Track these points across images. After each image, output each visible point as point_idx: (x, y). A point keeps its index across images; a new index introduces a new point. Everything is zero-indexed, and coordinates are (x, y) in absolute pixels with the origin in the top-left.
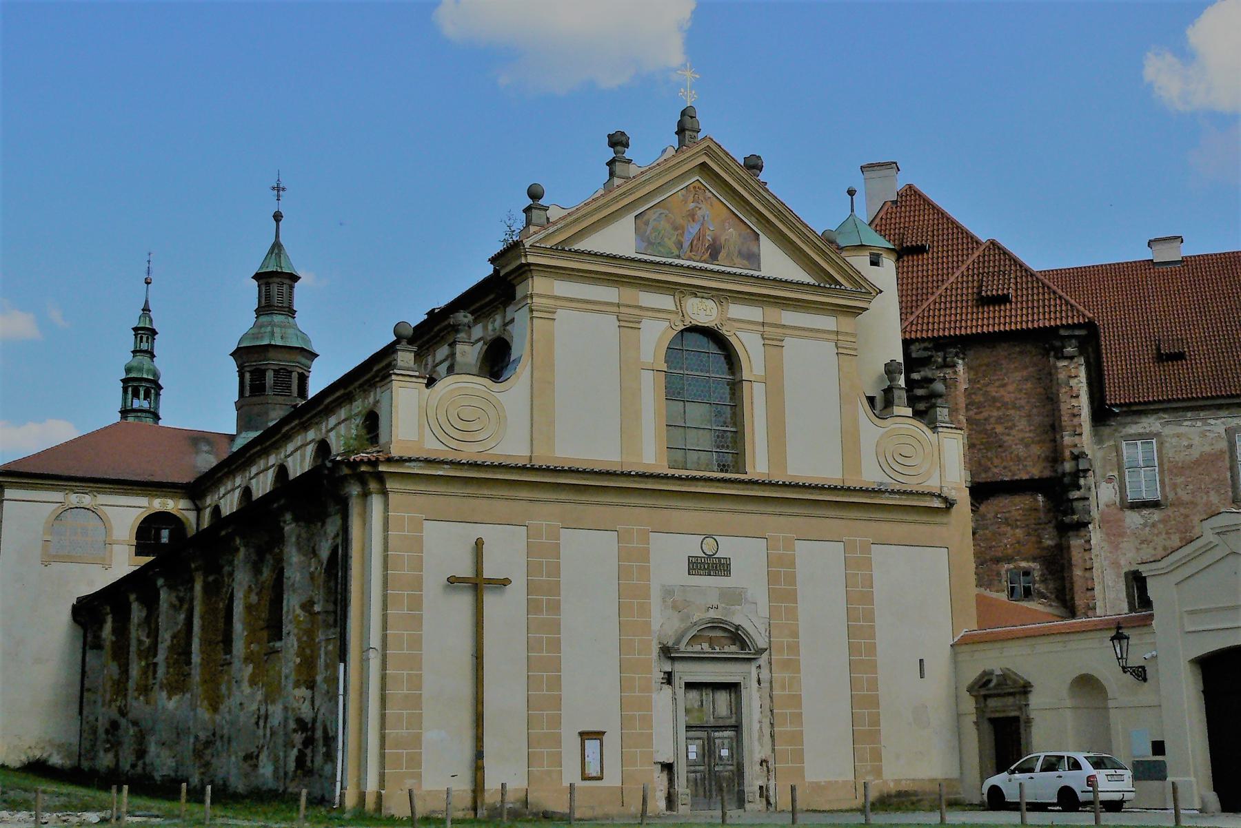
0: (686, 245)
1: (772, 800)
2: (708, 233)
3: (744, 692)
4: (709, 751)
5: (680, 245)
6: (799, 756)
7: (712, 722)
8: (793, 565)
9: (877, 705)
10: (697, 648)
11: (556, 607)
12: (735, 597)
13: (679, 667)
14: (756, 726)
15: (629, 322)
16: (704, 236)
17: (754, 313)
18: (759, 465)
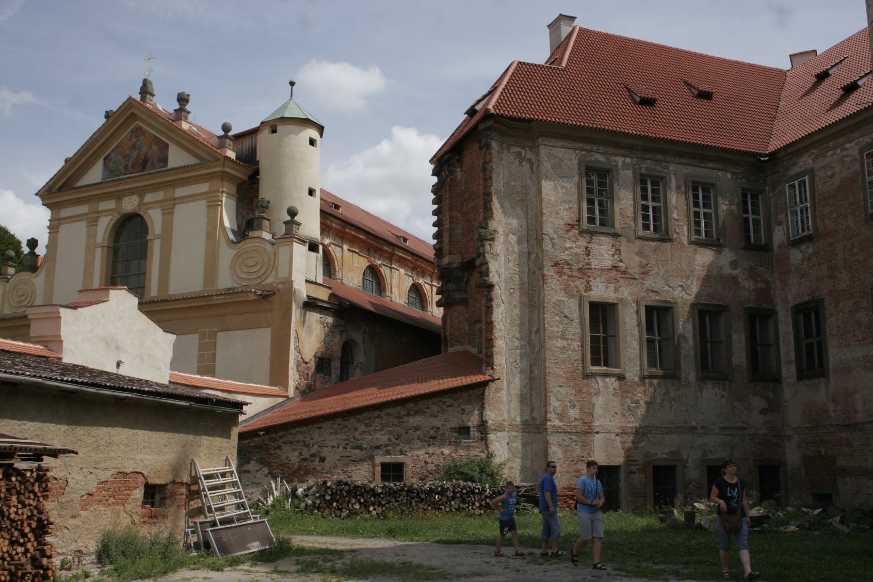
0: (130, 165)
15: (92, 223)
17: (160, 195)
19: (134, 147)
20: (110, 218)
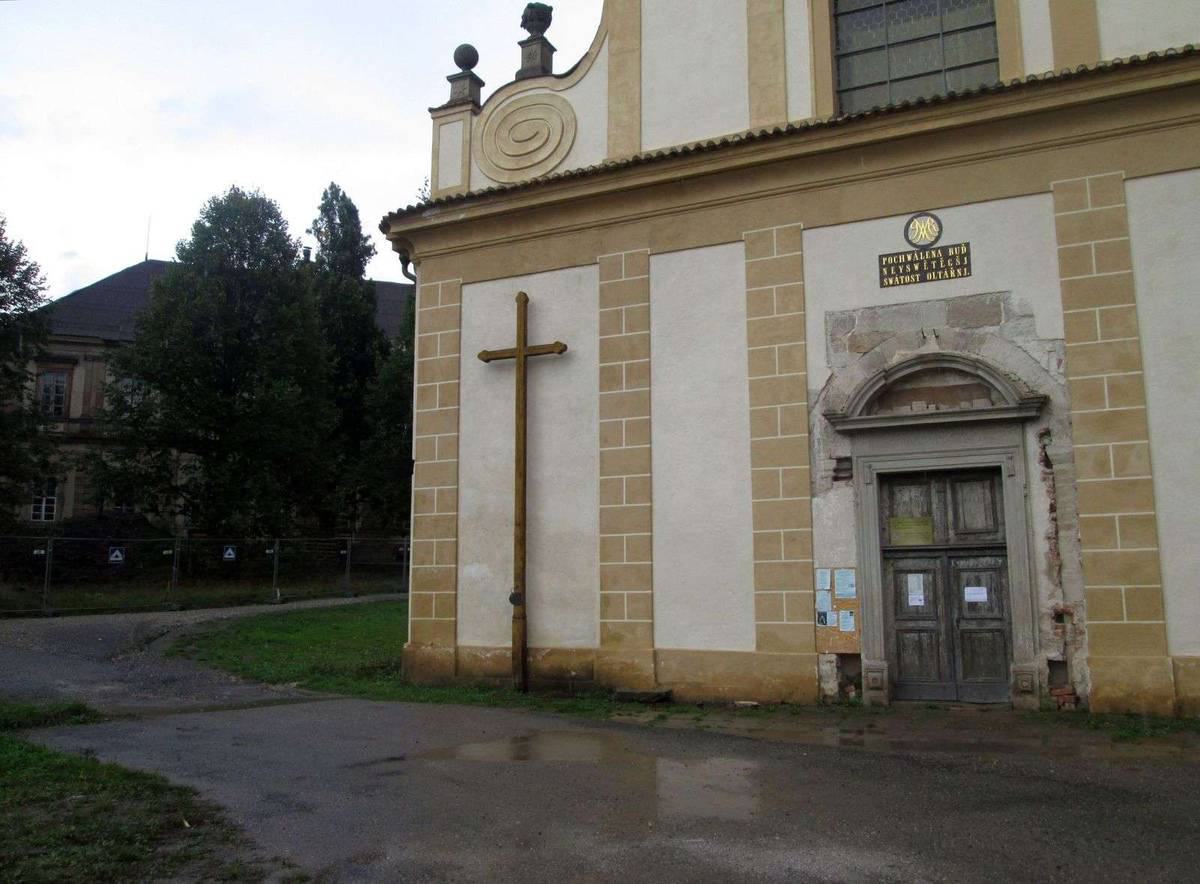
3: (1010, 487)
4: (946, 592)
6: (1153, 603)
8: (1120, 225)
10: (905, 410)
11: (644, 374)
12: (986, 310)
13: (864, 447)
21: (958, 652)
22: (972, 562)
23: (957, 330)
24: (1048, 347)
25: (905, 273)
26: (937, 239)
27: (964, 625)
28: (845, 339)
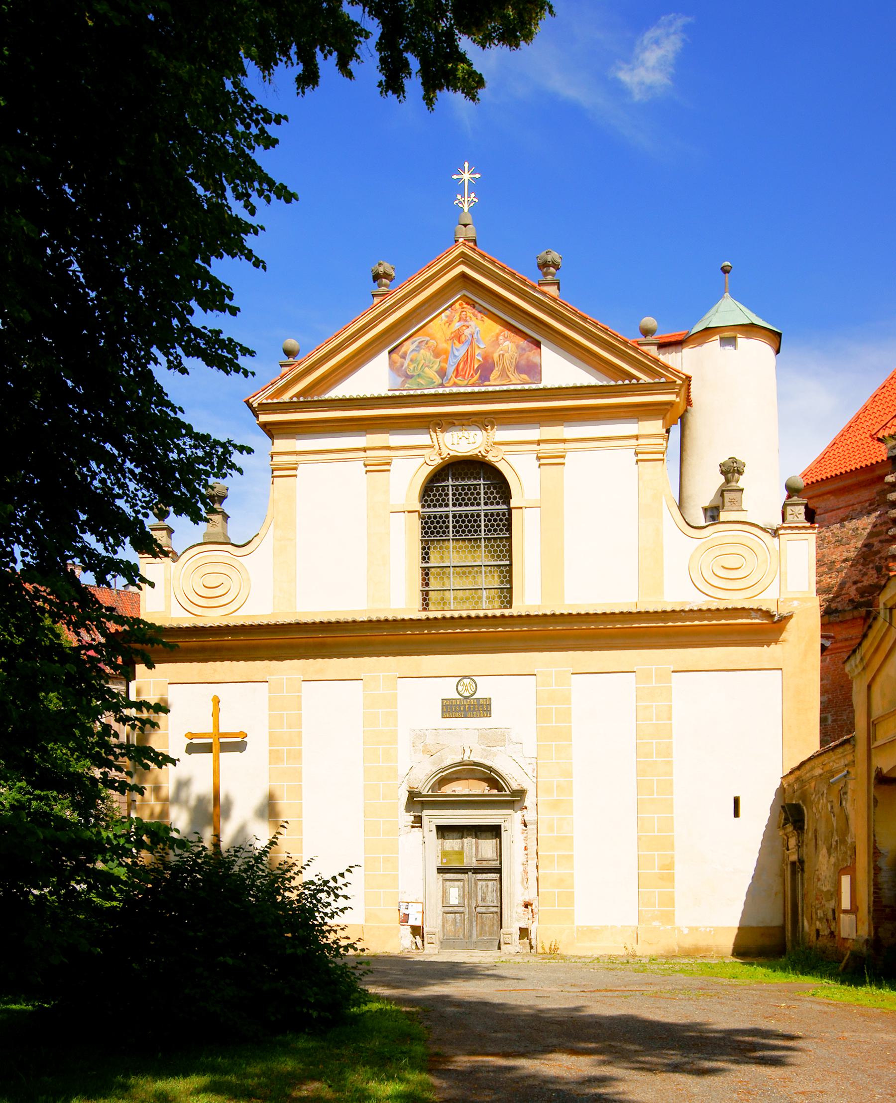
0: (451, 370)
1: (533, 943)
2: (477, 352)
5: (442, 373)
6: (569, 898)
7: (474, 864)
9: (672, 847)
11: (297, 756)
14: (518, 869)
16: (473, 357)
18: (529, 598)
19: (458, 337)
20: (422, 461)
21: (474, 924)
22: (484, 876)
23: (483, 747)
24: (529, 761)
25: (455, 710)
26: (472, 695)
27: (478, 909)
28: (421, 747)
